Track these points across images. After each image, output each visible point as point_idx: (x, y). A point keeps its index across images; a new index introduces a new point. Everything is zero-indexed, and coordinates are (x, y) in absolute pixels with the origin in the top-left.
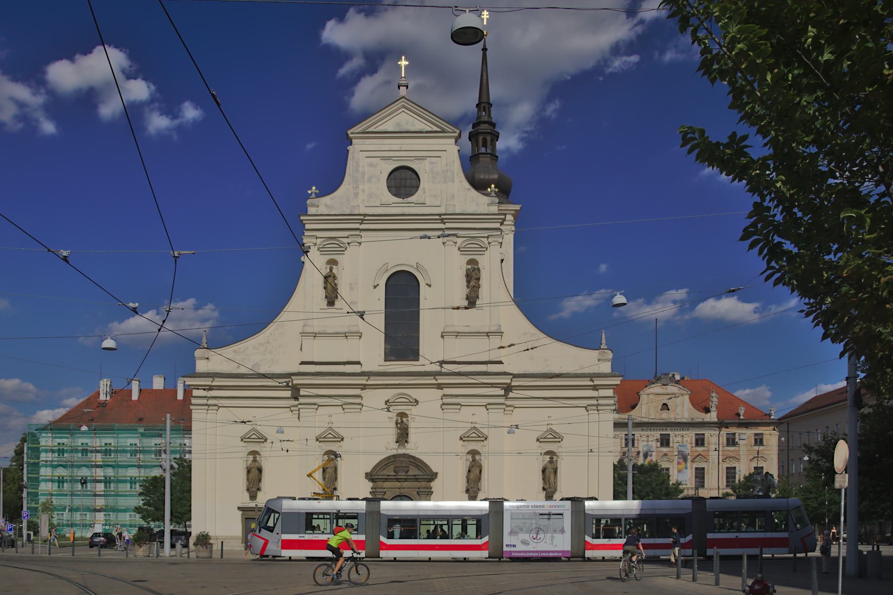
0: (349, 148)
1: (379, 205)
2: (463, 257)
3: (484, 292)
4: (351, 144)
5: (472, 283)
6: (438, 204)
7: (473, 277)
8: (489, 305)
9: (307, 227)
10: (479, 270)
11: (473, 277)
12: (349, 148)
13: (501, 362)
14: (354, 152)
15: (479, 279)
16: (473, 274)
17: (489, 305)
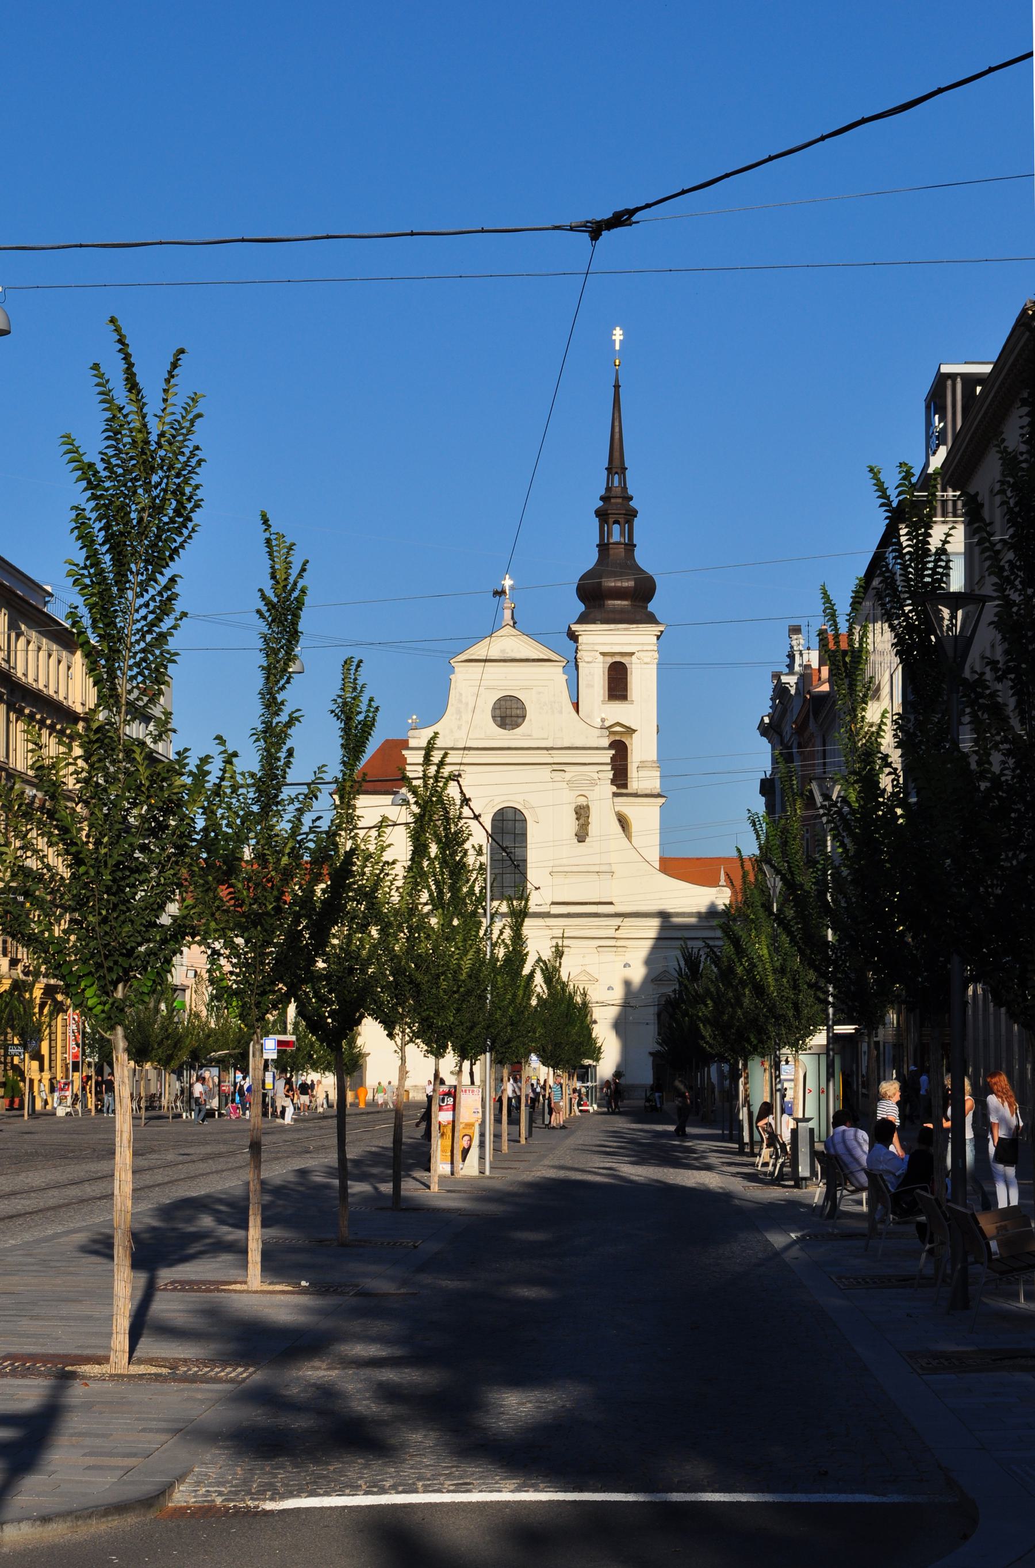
0: (452, 677)
1: (483, 736)
2: (572, 792)
3: (593, 829)
4: (453, 672)
5: (582, 821)
6: (546, 736)
7: (582, 813)
8: (603, 838)
9: (408, 762)
10: (588, 807)
11: (582, 813)
12: (452, 677)
13: (611, 903)
14: (456, 682)
15: (588, 817)
16: (582, 811)
17: (603, 838)
